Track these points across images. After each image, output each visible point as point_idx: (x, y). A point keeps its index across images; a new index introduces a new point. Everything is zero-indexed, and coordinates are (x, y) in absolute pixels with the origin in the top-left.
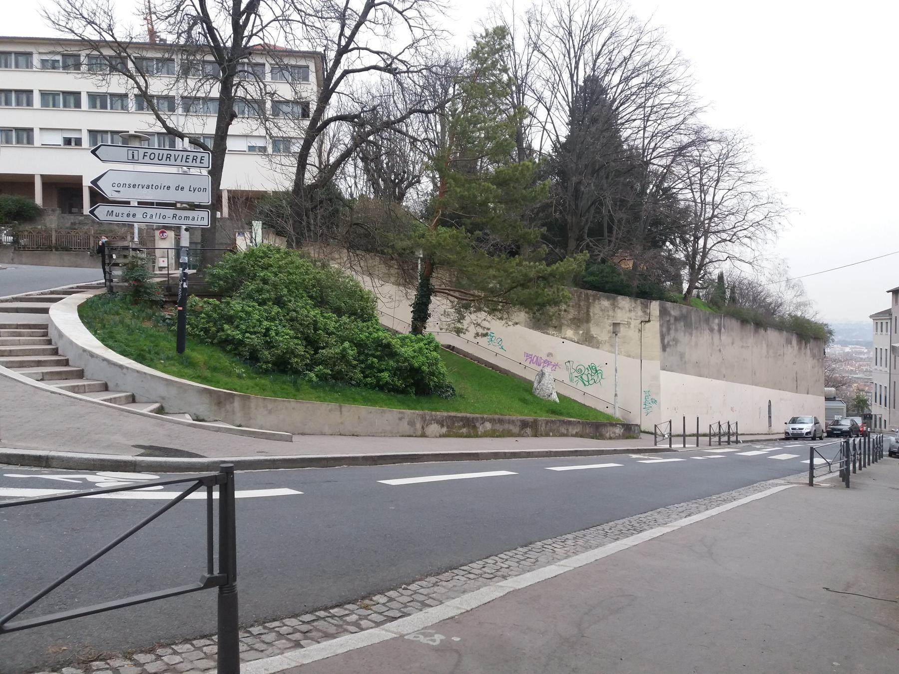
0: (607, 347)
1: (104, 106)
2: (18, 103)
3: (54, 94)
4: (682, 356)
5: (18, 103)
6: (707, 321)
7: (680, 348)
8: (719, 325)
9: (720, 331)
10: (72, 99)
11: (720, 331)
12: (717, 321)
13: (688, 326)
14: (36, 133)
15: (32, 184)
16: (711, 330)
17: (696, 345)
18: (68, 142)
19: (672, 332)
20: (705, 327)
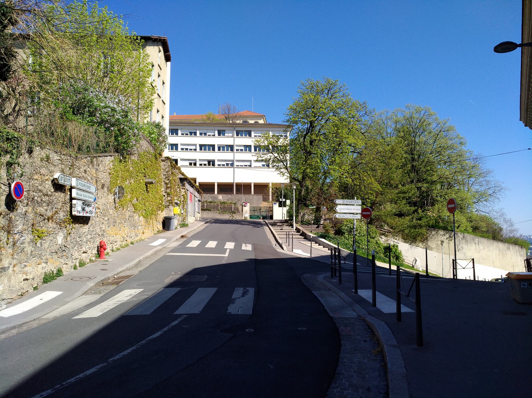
0: (435, 250)
1: (205, 149)
2: (209, 150)
3: (205, 146)
4: (465, 254)
5: (227, 150)
6: (473, 239)
7: (464, 251)
8: (478, 241)
9: (478, 243)
10: (231, 148)
11: (478, 243)
12: (477, 239)
13: (467, 241)
14: (179, 162)
15: (214, 185)
16: (475, 243)
17: (470, 249)
18: (191, 164)
19: (461, 244)
20: (473, 242)
